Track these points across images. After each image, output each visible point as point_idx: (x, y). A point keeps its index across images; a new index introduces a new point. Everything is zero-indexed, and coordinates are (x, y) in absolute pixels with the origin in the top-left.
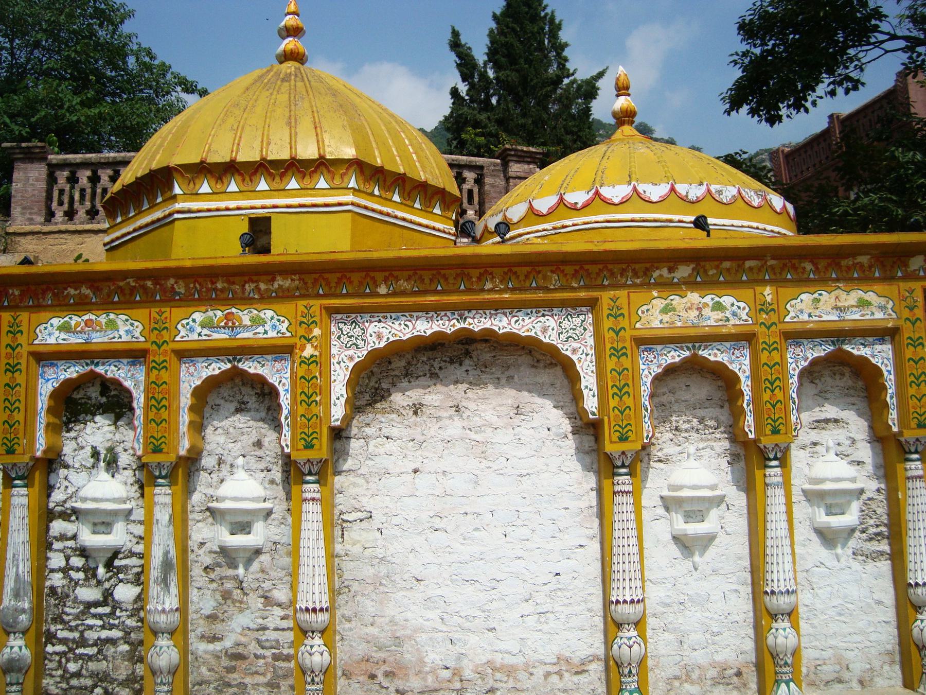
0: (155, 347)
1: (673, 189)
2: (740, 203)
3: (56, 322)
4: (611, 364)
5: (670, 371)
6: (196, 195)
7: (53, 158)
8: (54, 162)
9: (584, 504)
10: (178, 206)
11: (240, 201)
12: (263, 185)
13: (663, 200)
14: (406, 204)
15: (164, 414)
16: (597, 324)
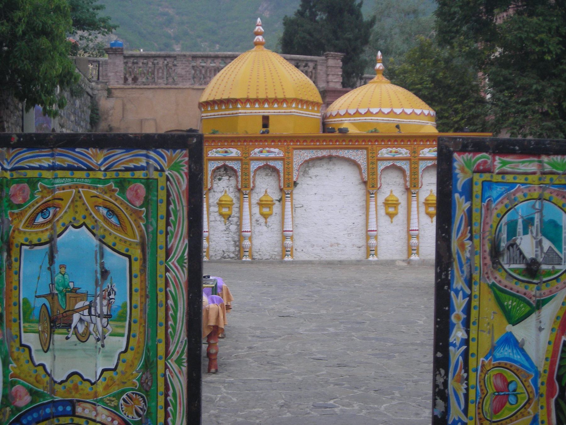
0: (244, 158)
1: (392, 110)
2: (413, 114)
3: (214, 150)
4: (371, 166)
5: (387, 168)
6: (245, 108)
7: (128, 53)
8: (127, 55)
9: (361, 204)
10: (240, 111)
11: (260, 111)
12: (266, 106)
13: (388, 113)
14: (307, 109)
15: (247, 177)
16: (368, 154)
